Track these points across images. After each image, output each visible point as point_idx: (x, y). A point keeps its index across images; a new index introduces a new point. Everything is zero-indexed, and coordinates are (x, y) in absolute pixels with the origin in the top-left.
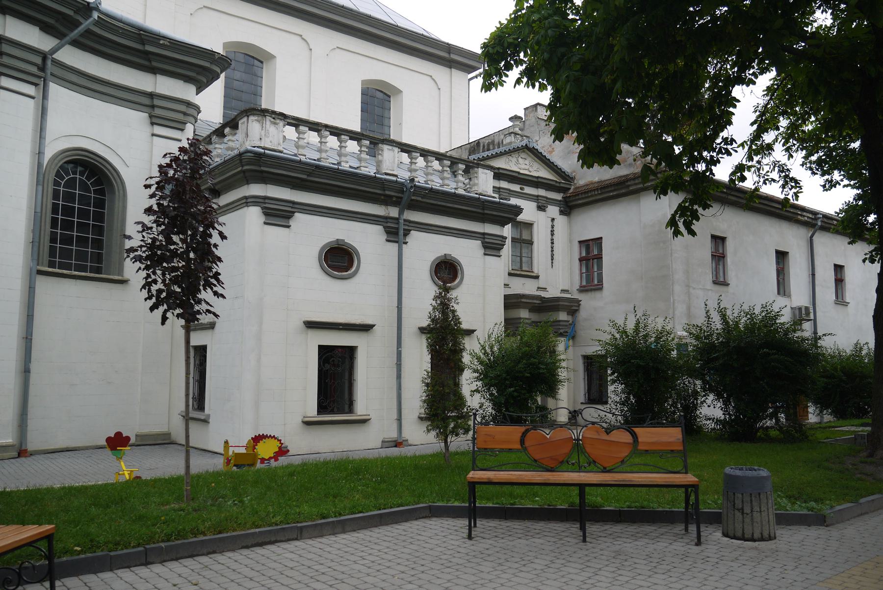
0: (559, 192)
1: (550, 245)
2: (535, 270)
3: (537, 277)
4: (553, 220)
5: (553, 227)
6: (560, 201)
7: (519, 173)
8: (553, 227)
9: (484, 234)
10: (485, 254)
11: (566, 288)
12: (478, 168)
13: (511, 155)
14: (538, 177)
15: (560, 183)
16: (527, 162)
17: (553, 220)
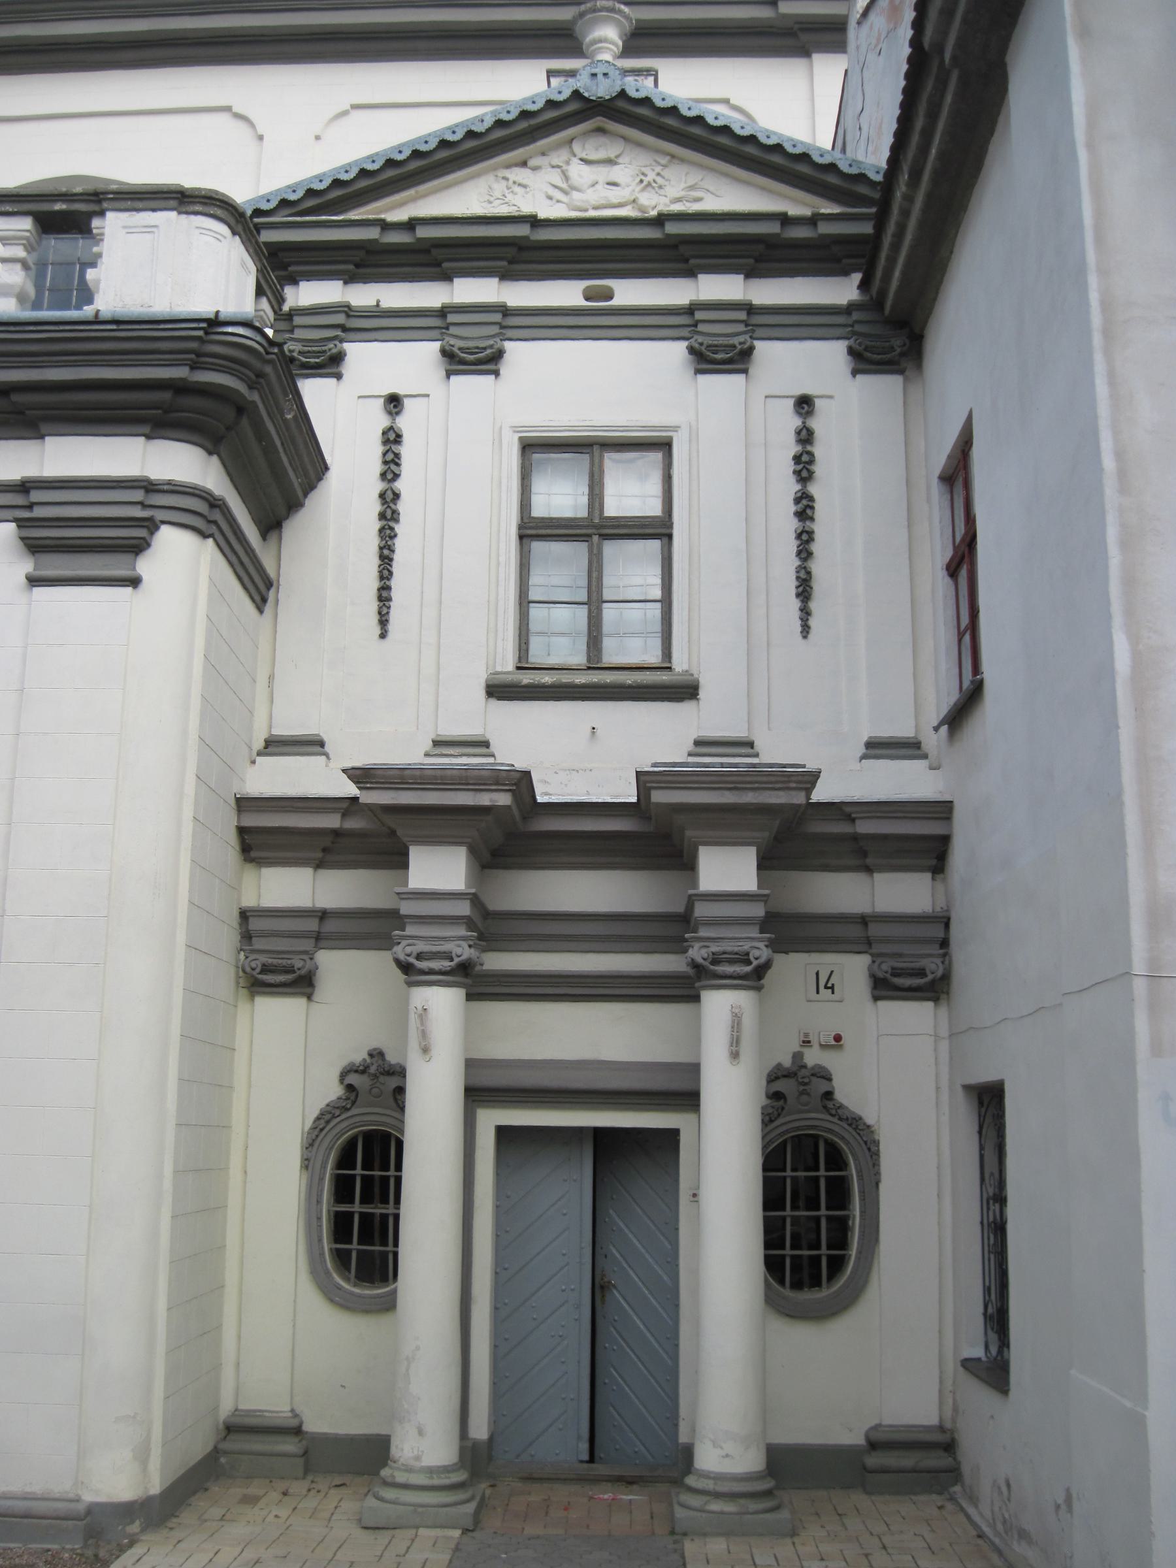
0: (845, 273)
1: (793, 524)
2: (680, 663)
3: (686, 691)
4: (804, 404)
5: (805, 437)
6: (850, 308)
7: (534, 221)
8: (805, 437)
9: (24, 487)
10: (34, 581)
11: (903, 729)
12: (102, 214)
13: (524, 164)
14: (660, 220)
15: (813, 220)
16: (619, 173)
17: (804, 404)
